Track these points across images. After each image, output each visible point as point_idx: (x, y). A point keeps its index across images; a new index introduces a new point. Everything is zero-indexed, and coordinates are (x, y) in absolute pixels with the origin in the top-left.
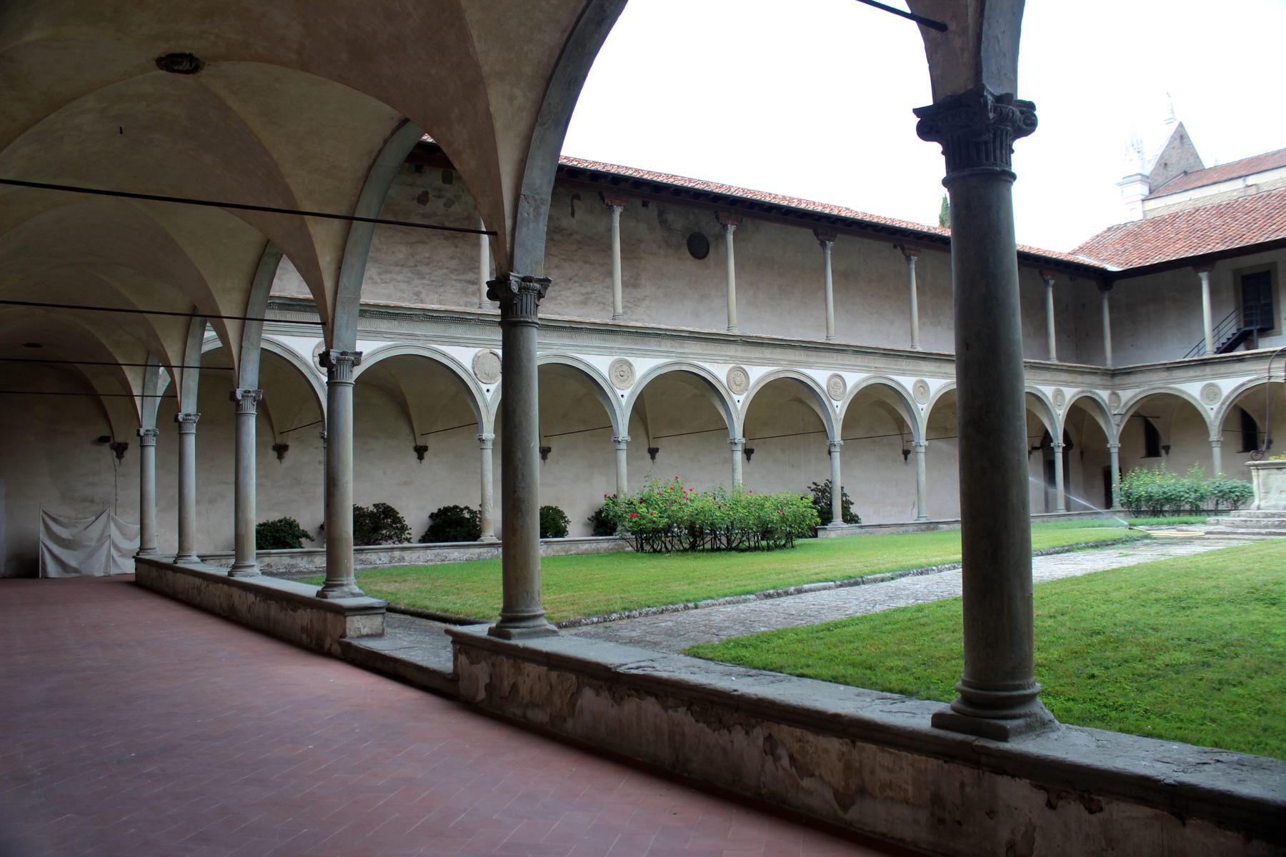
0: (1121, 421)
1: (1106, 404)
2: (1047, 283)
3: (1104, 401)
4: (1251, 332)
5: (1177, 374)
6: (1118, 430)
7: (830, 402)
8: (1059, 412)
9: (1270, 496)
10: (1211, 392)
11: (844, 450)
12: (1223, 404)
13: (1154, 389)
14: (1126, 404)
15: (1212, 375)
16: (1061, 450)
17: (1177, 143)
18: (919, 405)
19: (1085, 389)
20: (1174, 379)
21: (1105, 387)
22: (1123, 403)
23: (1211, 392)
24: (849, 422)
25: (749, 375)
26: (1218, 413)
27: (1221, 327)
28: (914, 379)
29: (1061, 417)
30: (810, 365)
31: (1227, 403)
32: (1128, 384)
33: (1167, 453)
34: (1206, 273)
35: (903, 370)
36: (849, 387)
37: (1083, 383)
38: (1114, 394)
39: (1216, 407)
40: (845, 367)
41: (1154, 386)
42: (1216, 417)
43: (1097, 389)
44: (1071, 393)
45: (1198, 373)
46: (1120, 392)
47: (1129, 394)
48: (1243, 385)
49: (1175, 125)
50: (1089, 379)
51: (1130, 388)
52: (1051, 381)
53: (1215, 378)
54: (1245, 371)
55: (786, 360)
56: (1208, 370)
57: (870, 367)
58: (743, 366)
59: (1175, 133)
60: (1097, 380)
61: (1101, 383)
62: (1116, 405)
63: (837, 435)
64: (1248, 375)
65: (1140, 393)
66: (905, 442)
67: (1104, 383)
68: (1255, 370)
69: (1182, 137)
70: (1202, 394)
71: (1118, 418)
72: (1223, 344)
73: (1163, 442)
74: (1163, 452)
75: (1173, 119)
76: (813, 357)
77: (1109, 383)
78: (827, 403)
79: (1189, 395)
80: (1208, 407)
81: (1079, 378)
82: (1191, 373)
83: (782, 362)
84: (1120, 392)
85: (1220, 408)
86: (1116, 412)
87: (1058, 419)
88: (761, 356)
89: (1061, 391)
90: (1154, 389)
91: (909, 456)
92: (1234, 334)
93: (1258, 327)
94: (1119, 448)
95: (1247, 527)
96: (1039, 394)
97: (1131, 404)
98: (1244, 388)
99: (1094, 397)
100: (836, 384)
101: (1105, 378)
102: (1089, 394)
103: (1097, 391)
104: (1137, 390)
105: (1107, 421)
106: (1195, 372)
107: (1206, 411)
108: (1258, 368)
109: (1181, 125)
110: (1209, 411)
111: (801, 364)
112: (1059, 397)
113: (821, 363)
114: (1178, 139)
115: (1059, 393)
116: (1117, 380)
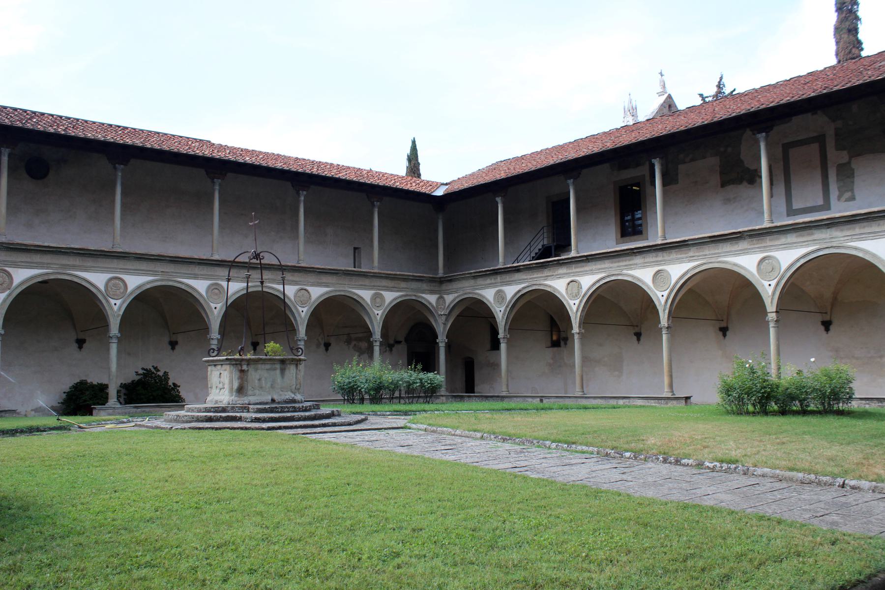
0: (446, 320)
1: (432, 306)
2: (373, 206)
3: (430, 303)
5: (480, 281)
6: (444, 329)
7: (107, 301)
8: (376, 312)
10: (500, 296)
11: (120, 340)
13: (466, 294)
14: (448, 307)
15: (501, 283)
16: (378, 344)
17: (666, 111)
18: (212, 304)
19: (410, 293)
20: (478, 286)
21: (432, 292)
23: (500, 296)
24: (127, 318)
25: (13, 276)
27: (532, 244)
28: (208, 283)
29: (378, 317)
30: (86, 269)
31: (510, 306)
35: (195, 274)
36: (130, 289)
37: (408, 288)
38: (441, 298)
39: (503, 309)
40: (127, 271)
42: (503, 317)
43: (423, 293)
44: (390, 297)
45: (493, 281)
46: (445, 296)
47: (450, 299)
48: (519, 291)
49: (666, 96)
50: (414, 285)
52: (371, 286)
53: (502, 285)
54: (521, 280)
55: (58, 264)
56: (499, 278)
57: (156, 271)
58: (7, 269)
59: (664, 102)
60: (425, 286)
61: (428, 288)
62: (443, 307)
63: (114, 328)
64: (520, 283)
67: (432, 288)
68: (527, 279)
69: (670, 106)
71: (444, 318)
75: (664, 92)
76: (89, 262)
77: (436, 289)
78: (104, 301)
79: (487, 299)
80: (498, 310)
81: (403, 285)
82: (488, 281)
83: (52, 266)
84: (445, 296)
85: (505, 310)
87: (376, 318)
88: (29, 260)
89: (381, 294)
90: (466, 294)
91: (258, 348)
92: (539, 250)
94: (446, 343)
96: (355, 297)
97: (451, 306)
98: (520, 294)
99: (420, 300)
100: (115, 285)
101: (434, 284)
102: (414, 298)
103: (424, 295)
104: (456, 295)
105: (436, 320)
106: (491, 279)
107: (497, 312)
108: (529, 277)
109: (670, 97)
110: (499, 312)
111: (74, 267)
112: (378, 300)
113: (98, 267)
114: (668, 107)
115: (375, 297)
116: (444, 287)
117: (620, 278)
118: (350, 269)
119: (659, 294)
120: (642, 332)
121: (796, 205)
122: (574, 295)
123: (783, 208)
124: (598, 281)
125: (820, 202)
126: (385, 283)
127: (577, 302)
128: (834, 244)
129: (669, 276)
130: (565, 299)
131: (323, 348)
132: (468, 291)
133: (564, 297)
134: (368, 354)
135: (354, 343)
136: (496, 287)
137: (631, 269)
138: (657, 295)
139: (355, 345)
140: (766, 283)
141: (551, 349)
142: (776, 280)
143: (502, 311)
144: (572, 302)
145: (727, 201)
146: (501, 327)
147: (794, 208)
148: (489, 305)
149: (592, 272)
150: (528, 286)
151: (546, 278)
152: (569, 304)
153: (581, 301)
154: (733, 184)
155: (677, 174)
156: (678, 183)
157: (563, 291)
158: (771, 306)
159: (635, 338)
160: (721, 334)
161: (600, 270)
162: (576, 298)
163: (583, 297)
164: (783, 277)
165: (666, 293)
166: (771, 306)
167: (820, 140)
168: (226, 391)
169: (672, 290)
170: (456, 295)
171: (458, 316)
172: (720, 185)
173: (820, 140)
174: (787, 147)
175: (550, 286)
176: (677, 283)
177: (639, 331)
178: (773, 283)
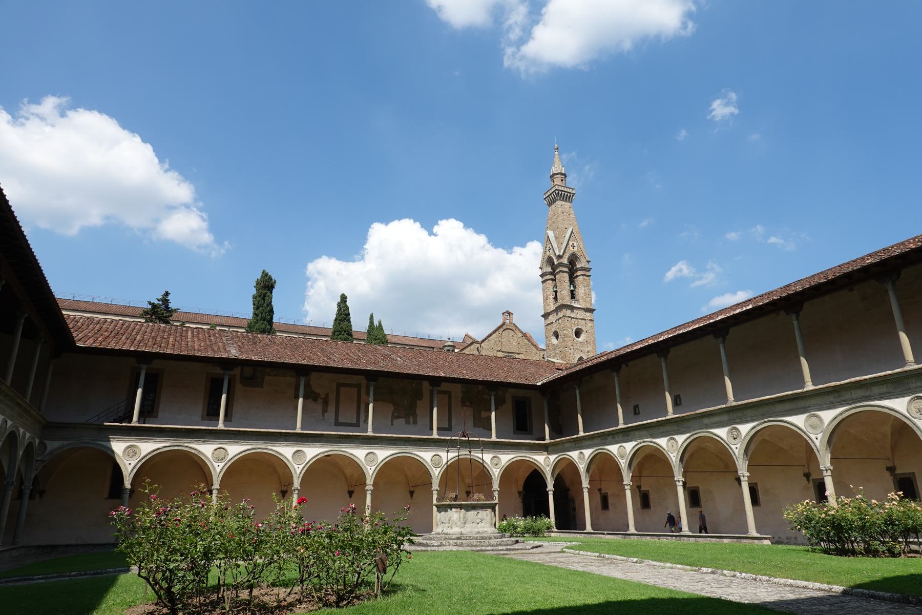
9: (466, 525)
22: (48, 450)
33: (41, 496)
39: (133, 463)
46: (47, 442)
72: (120, 417)
84: (47, 442)
86: (39, 459)
95: (483, 546)
104: (66, 442)
107: (125, 465)
110: (128, 465)
119: (296, 466)
121: (341, 420)
122: (220, 458)
123: (333, 420)
125: (354, 421)
127: (222, 465)
128: (407, 451)
138: (294, 467)
140: (369, 468)
142: (375, 467)
144: (216, 465)
147: (339, 421)
155: (263, 382)
158: (370, 481)
162: (221, 461)
163: (229, 461)
164: (379, 465)
166: (370, 481)
167: (358, 386)
168: (488, 525)
169: (306, 465)
173: (358, 386)
174: (339, 385)
178: (373, 468)
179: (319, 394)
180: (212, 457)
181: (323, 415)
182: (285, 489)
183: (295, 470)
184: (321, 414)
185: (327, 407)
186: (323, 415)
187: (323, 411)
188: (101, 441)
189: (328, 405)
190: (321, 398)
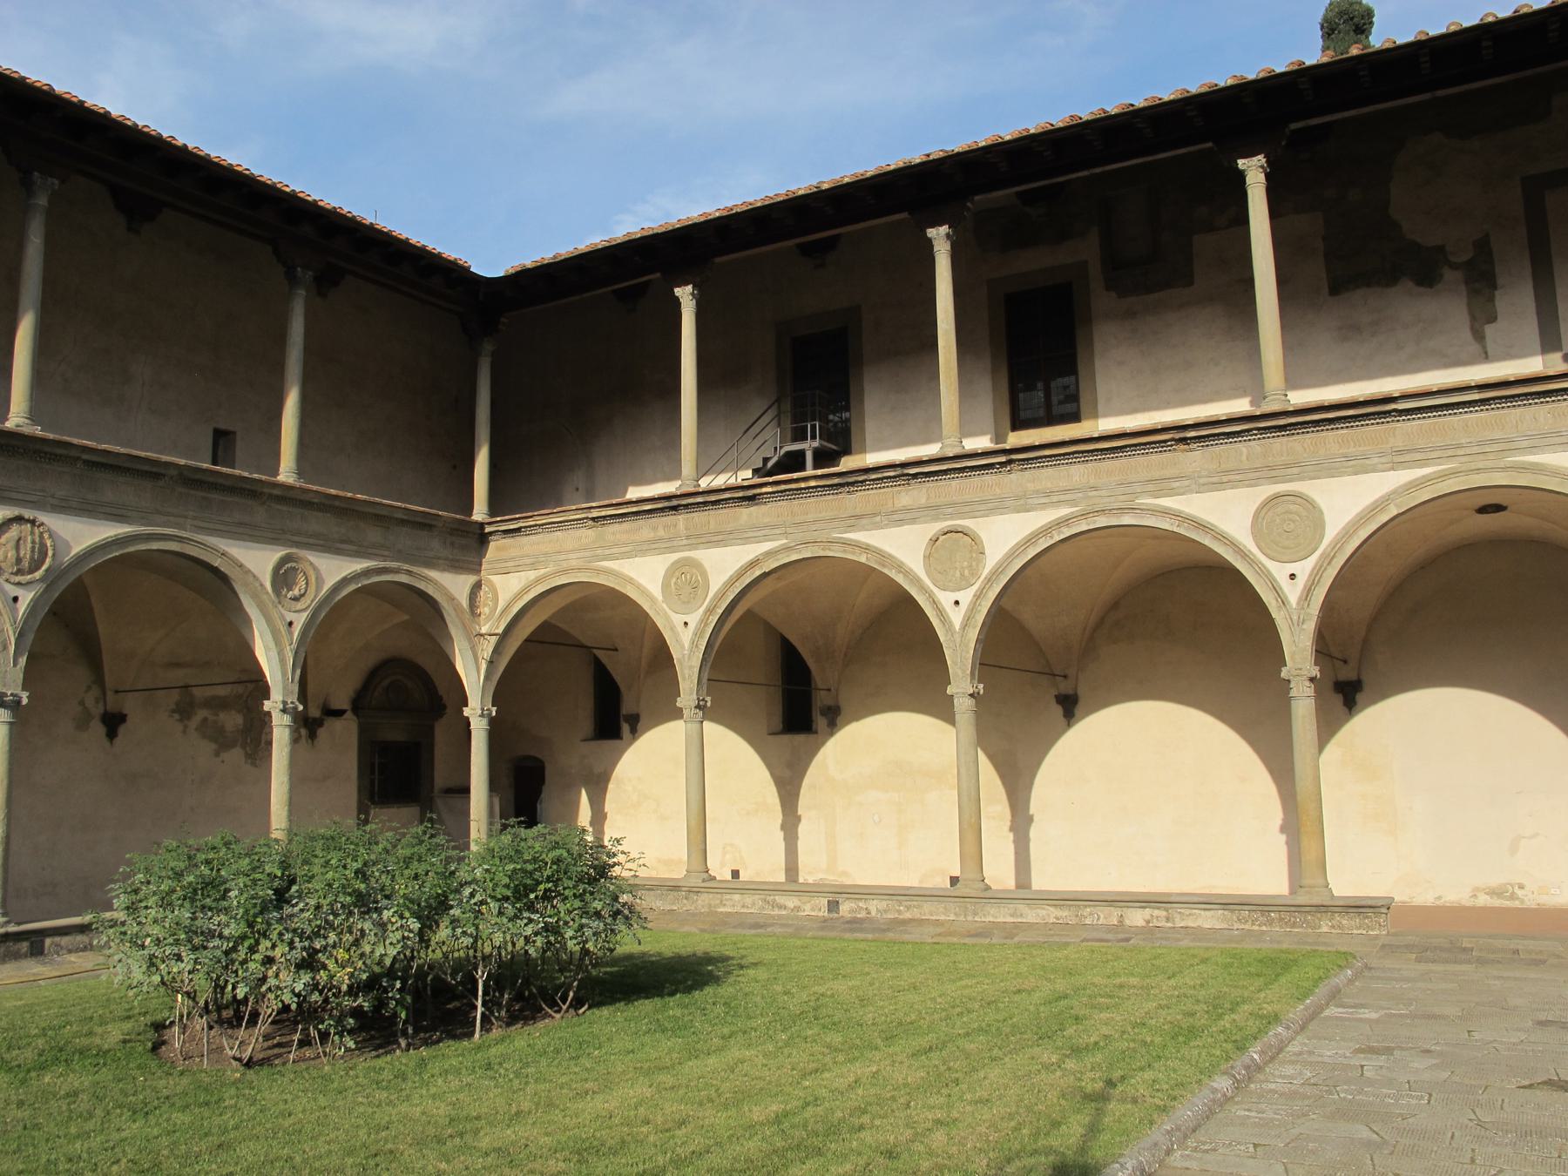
4: (802, 453)
12: (710, 611)
13: (565, 572)
23: (685, 580)
26: (698, 633)
32: (512, 559)
34: (689, 288)
39: (694, 619)
41: (565, 565)
51: (518, 569)
65: (538, 581)
66: (109, 694)
70: (665, 586)
73: (627, 708)
74: (625, 728)
79: (639, 587)
85: (704, 622)
90: (565, 572)
93: (816, 444)
102: (404, 579)
104: (532, 575)
107: (673, 628)
110: (680, 627)
117: (1127, 520)
118: (205, 466)
119: (1280, 571)
120: (1080, 693)
124: (1046, 530)
126: (317, 523)
127: (966, 597)
129: (1314, 516)
130: (923, 588)
131: (98, 729)
132: (574, 563)
133: (916, 580)
134: (243, 747)
135: (201, 714)
136: (672, 550)
137: (1172, 493)
139: (205, 720)
141: (786, 738)
143: (692, 626)
145: (1350, 331)
146: (686, 672)
148: (646, 606)
149: (1022, 505)
150: (787, 549)
151: (856, 520)
152: (935, 603)
153: (978, 596)
154: (1369, 285)
156: (1191, 283)
157: (916, 564)
159: (1058, 710)
160: (1338, 700)
161: (1049, 498)
163: (990, 580)
165: (1304, 568)
170: (532, 575)
171: (526, 640)
172: (1326, 290)
175: (866, 548)
176: (1347, 533)
177: (1071, 692)
179: (1441, 249)
180: (928, 573)
181: (1479, 336)
182: (1352, 676)
183: (1276, 589)
184: (1467, 335)
185: (1491, 299)
186: (1479, 336)
187: (1473, 318)
188: (606, 558)
189: (1494, 287)
190: (1454, 266)
